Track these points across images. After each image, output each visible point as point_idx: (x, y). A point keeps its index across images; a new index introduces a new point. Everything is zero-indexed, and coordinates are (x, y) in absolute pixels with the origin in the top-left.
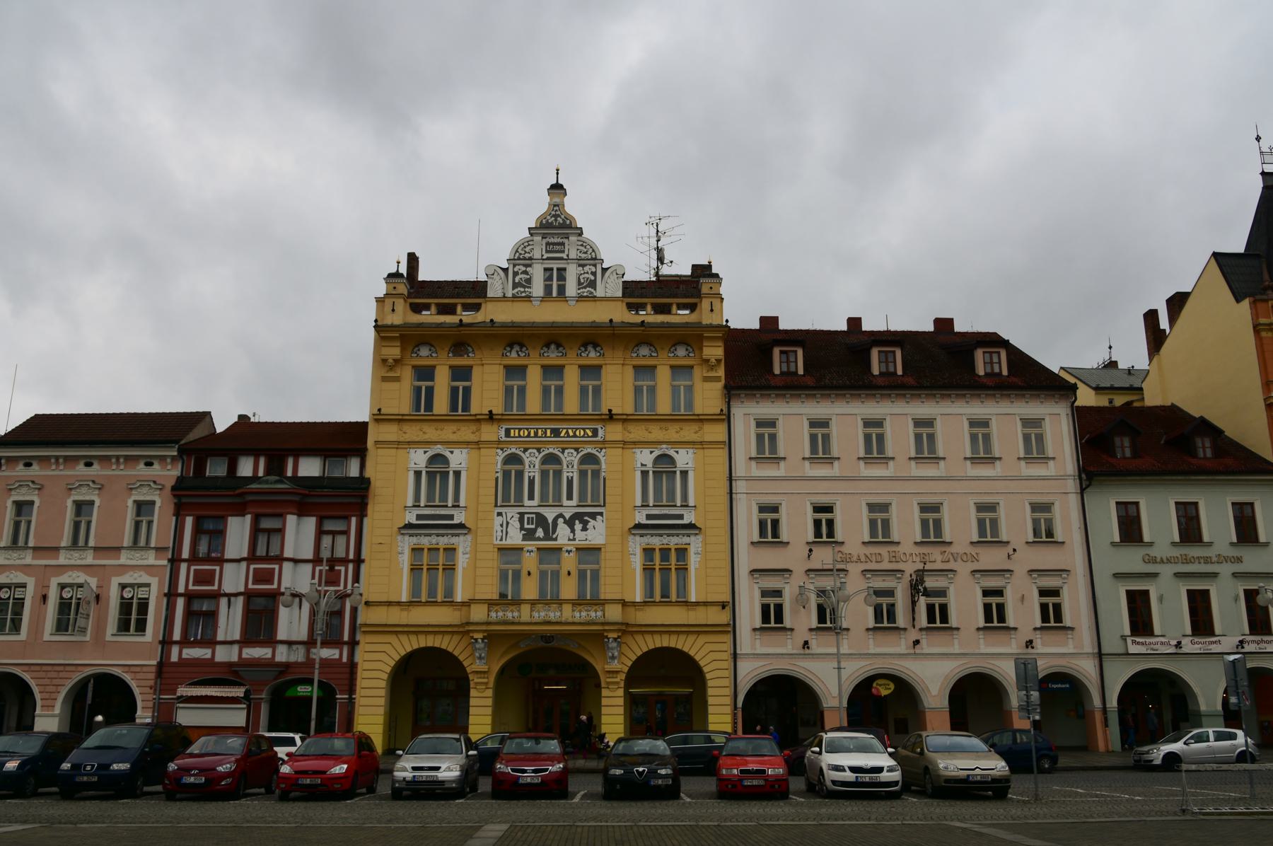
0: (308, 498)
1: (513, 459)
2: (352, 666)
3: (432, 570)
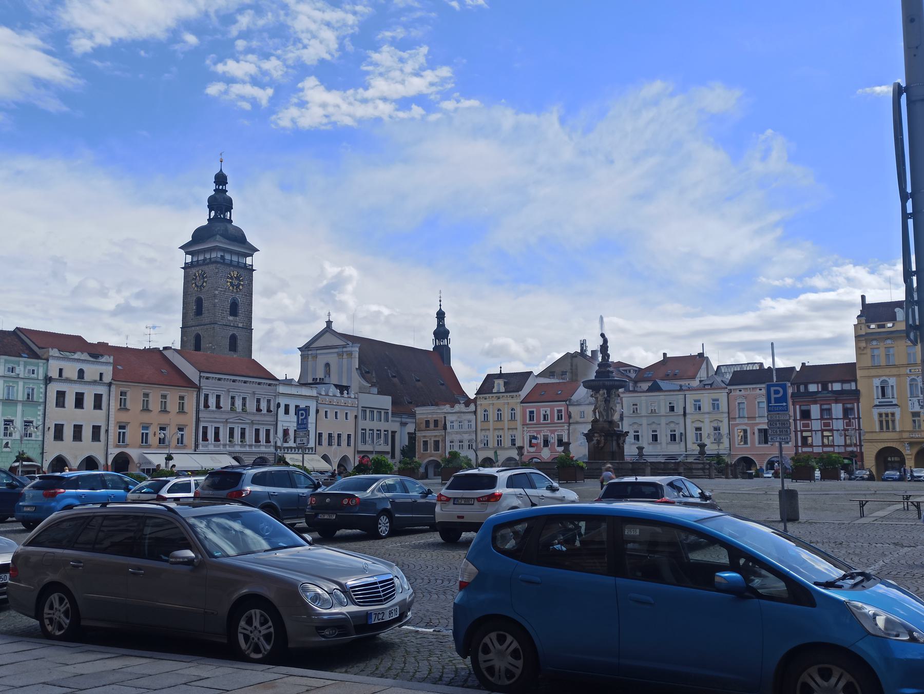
0: (838, 396)
1: (913, 380)
2: (862, 453)
3: (886, 422)
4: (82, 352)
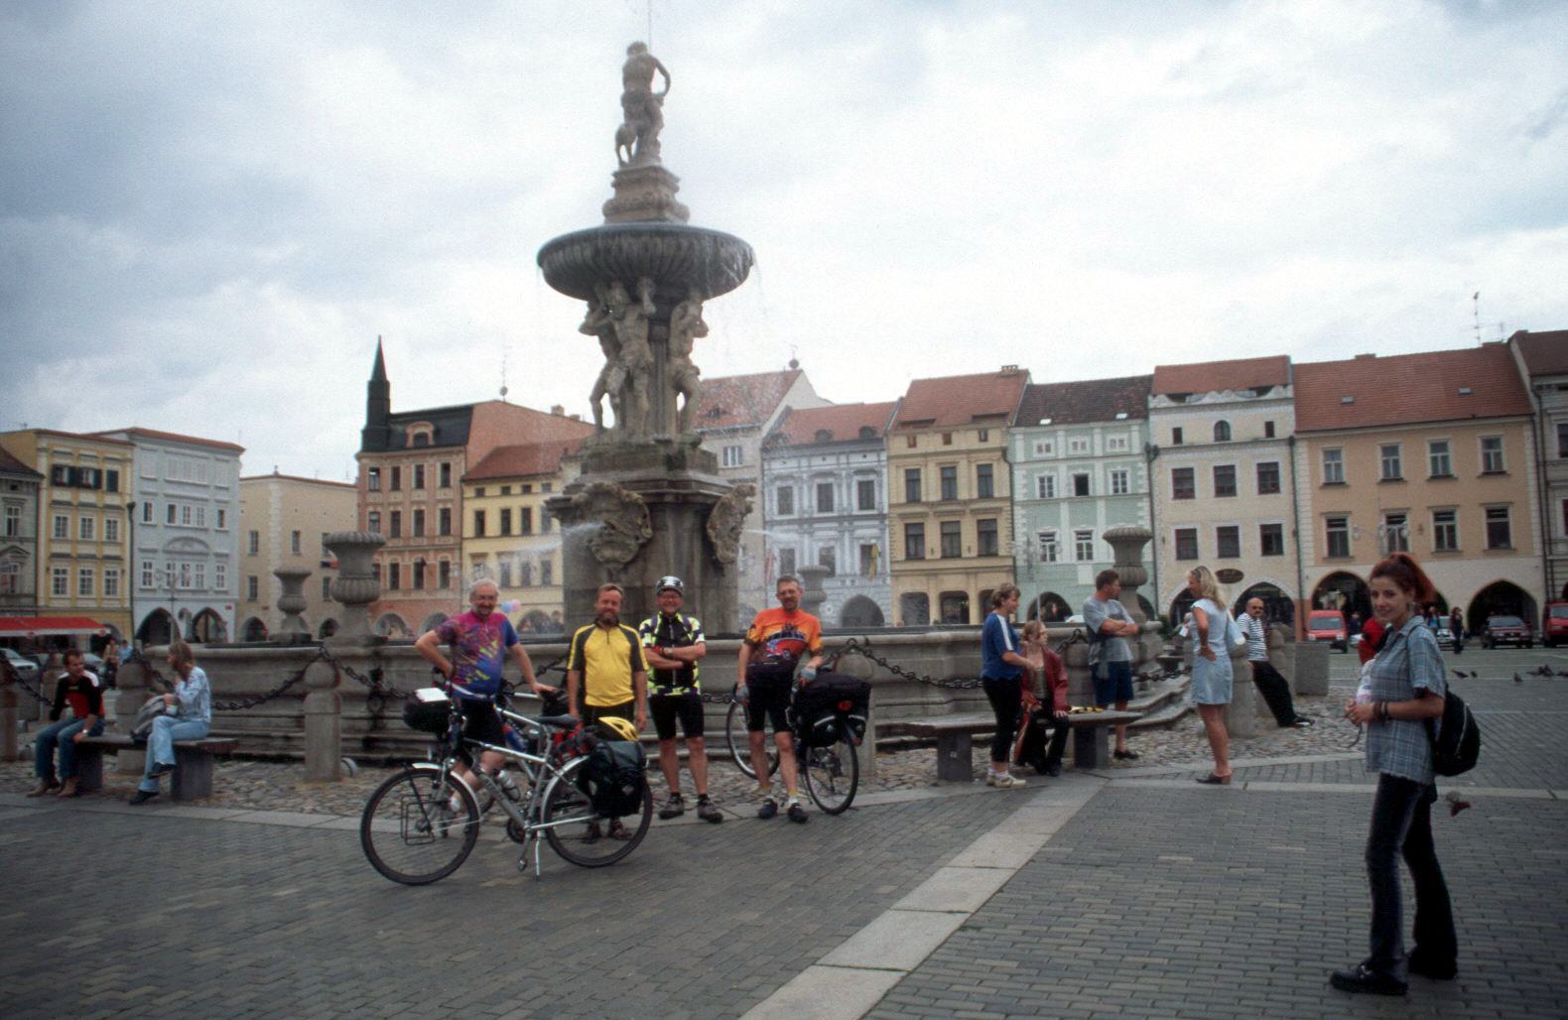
4: (1220, 391)
